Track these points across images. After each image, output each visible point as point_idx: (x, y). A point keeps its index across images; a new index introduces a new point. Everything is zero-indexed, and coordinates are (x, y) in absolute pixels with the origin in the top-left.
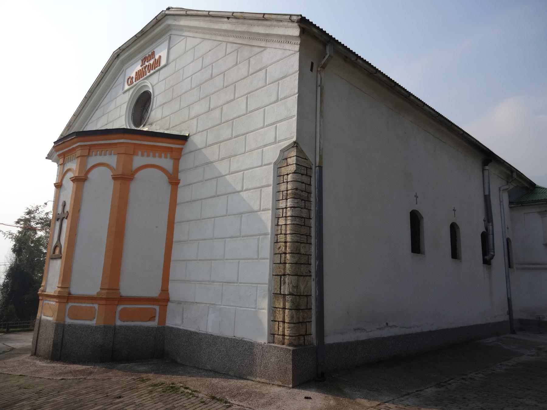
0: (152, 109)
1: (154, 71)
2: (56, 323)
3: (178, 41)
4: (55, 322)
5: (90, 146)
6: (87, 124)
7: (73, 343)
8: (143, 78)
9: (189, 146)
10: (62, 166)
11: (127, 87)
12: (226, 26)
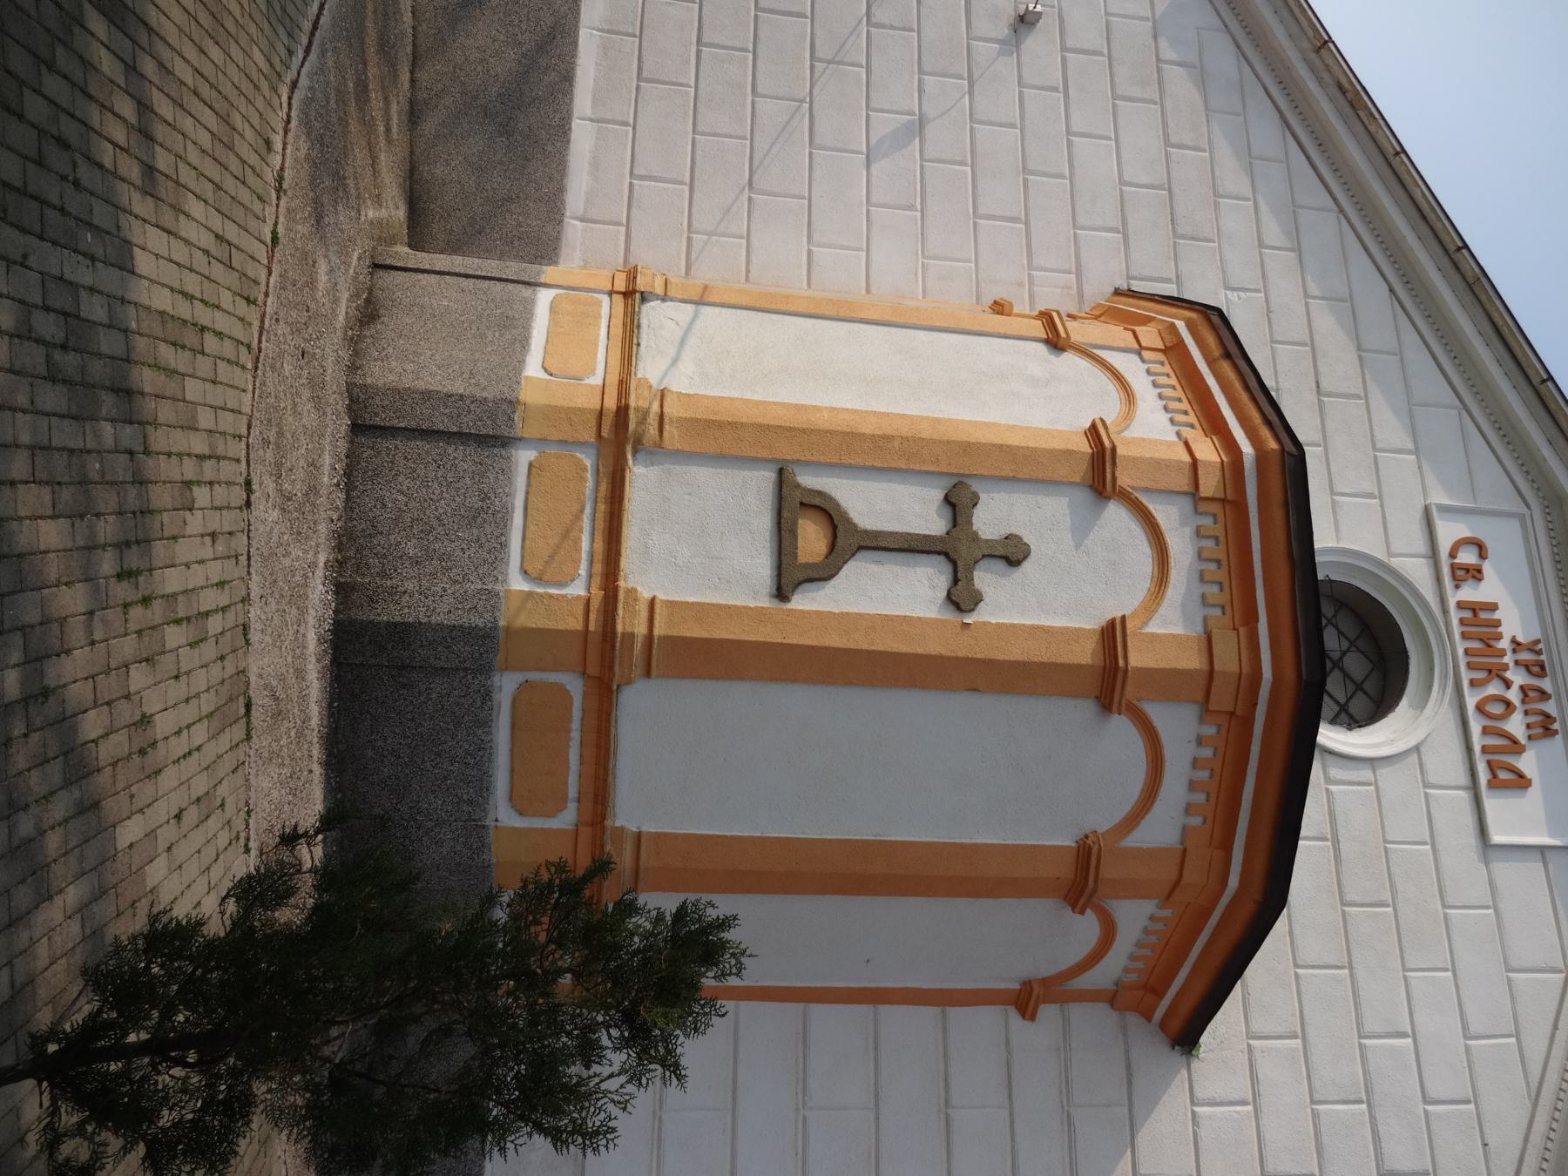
0: (1328, 756)
1: (1477, 741)
2: (495, 628)
3: (1559, 906)
4: (502, 623)
5: (1248, 722)
6: (1341, 210)
7: (413, 720)
8: (1463, 668)
9: (1150, 1048)
10: (1184, 483)
11: (1448, 532)
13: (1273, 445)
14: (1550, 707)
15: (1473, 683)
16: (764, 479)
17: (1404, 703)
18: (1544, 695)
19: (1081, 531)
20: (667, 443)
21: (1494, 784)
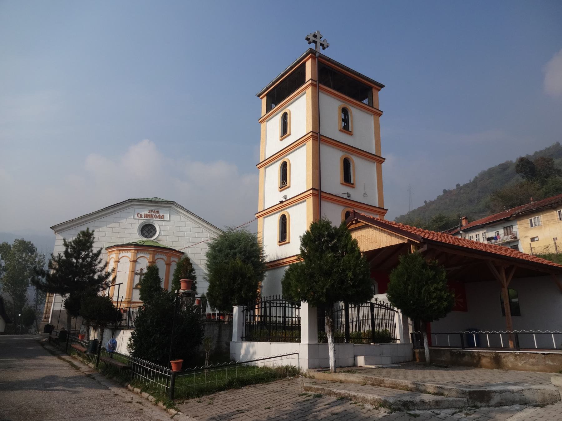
12: (205, 225)
13: (133, 246)
14: (156, 211)
15: (153, 218)
16: (134, 290)
17: (154, 225)
18: (155, 211)
19: (140, 264)
20: (131, 298)
21: (163, 218)
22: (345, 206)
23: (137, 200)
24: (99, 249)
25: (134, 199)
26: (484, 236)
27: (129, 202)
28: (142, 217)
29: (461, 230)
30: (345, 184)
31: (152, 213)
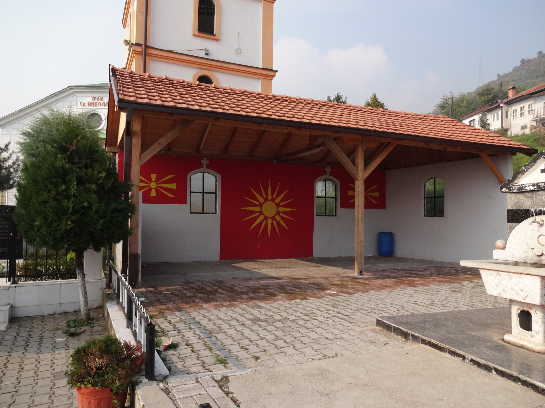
1: (104, 107)
14: (100, 97)
15: (97, 106)
18: (98, 98)
22: (199, 68)
23: (78, 87)
24: (7, 143)
25: (74, 86)
26: (530, 109)
27: (70, 89)
28: (85, 106)
29: (502, 102)
30: (200, 35)
31: (96, 101)
